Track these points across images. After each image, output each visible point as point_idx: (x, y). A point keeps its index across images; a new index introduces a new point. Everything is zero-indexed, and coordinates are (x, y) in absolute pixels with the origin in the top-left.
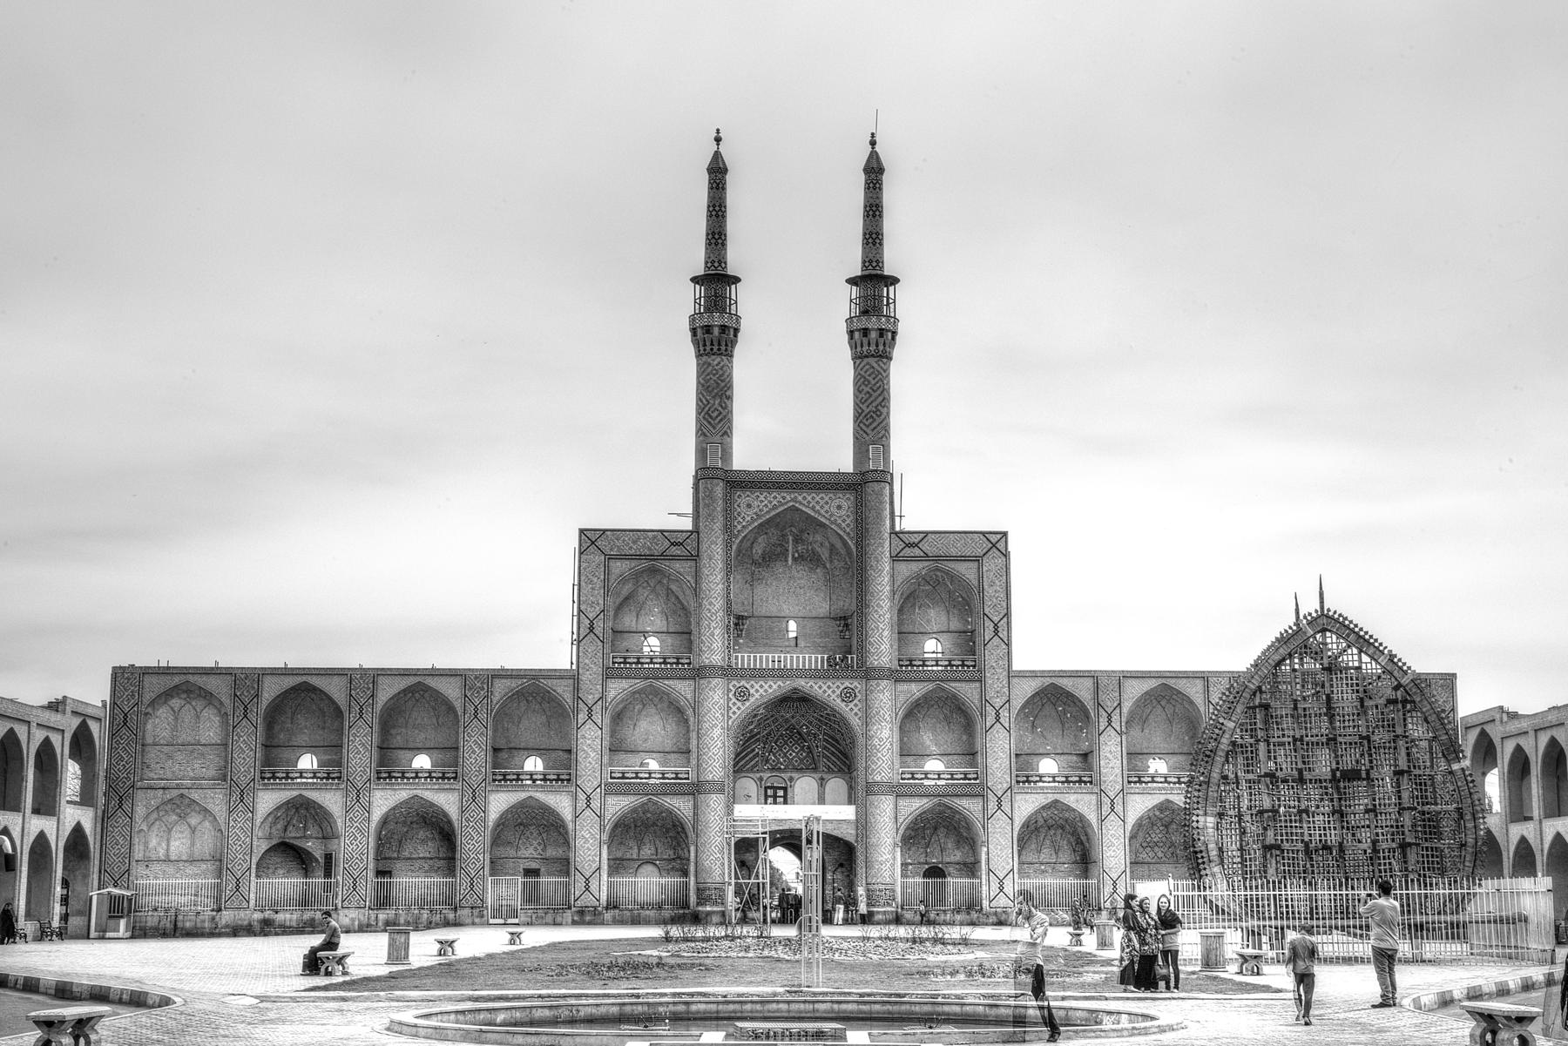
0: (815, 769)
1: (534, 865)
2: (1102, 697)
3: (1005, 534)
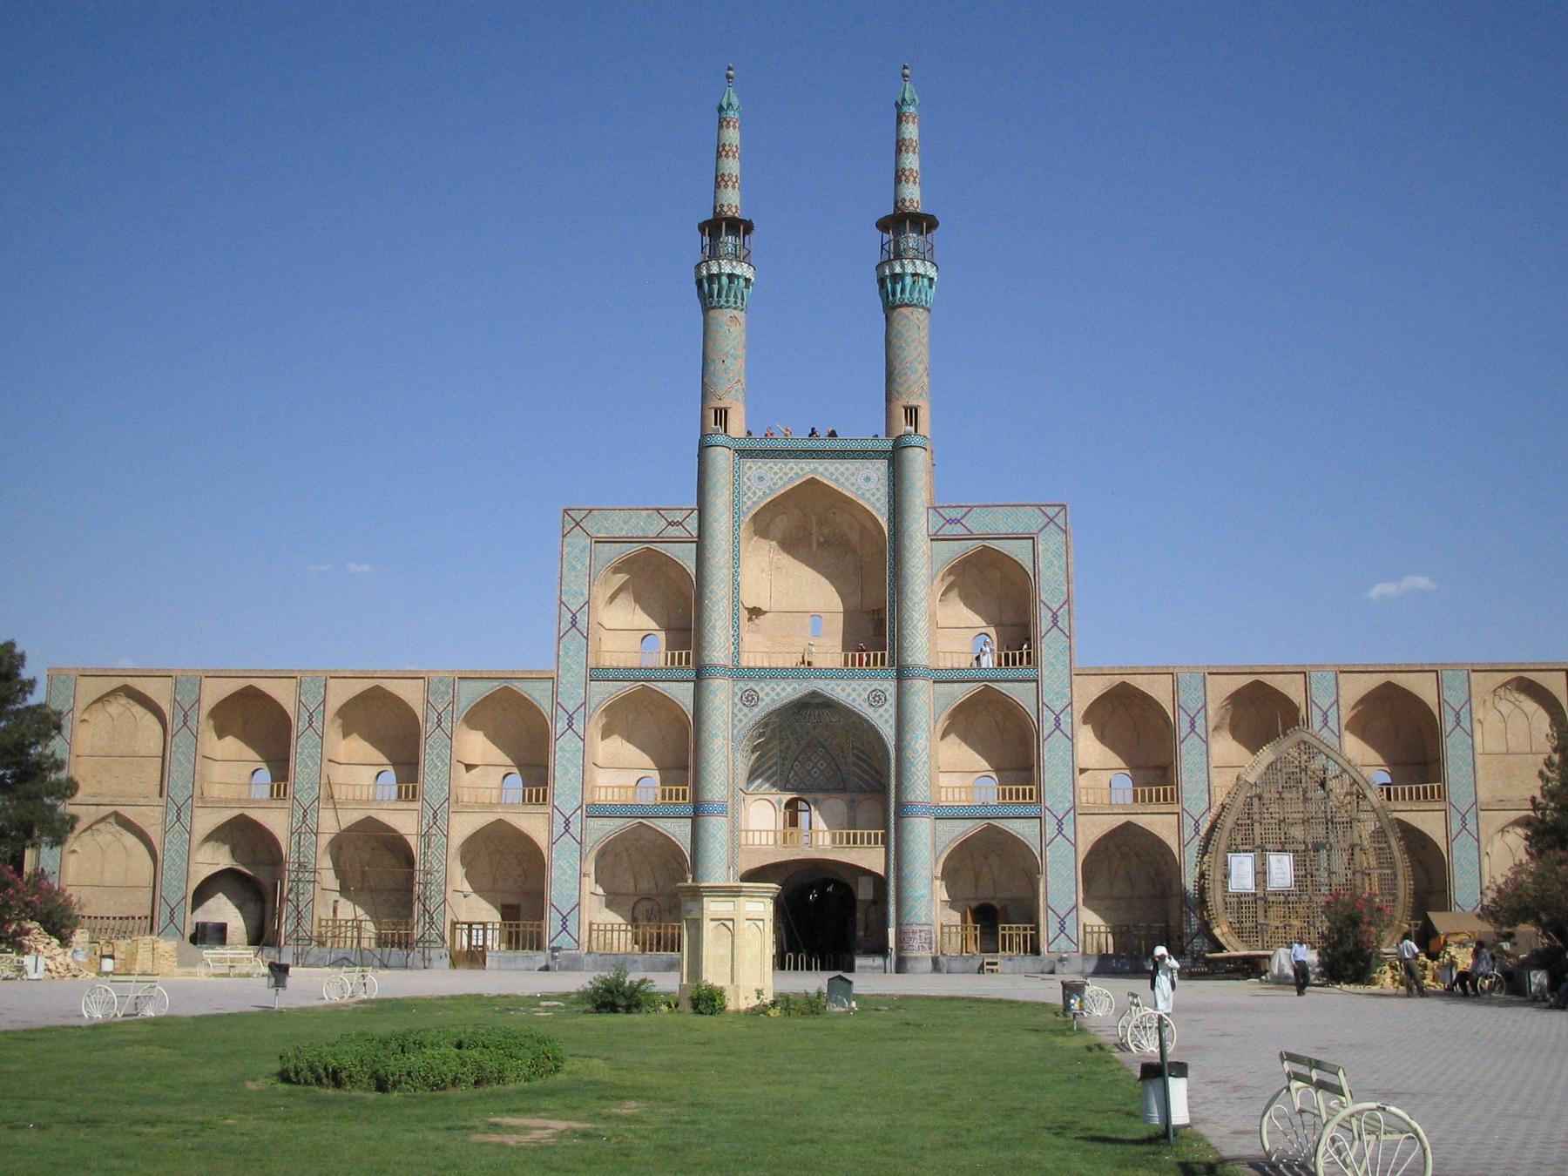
2: (1183, 698)
3: (1064, 506)
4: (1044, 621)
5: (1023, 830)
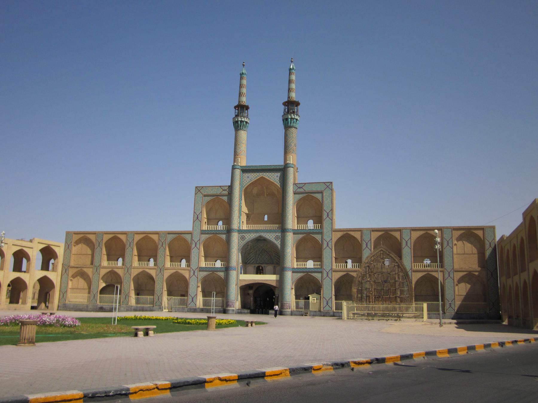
0: (273, 263)
1: (183, 293)
2: (364, 237)
4: (325, 216)
5: (318, 276)
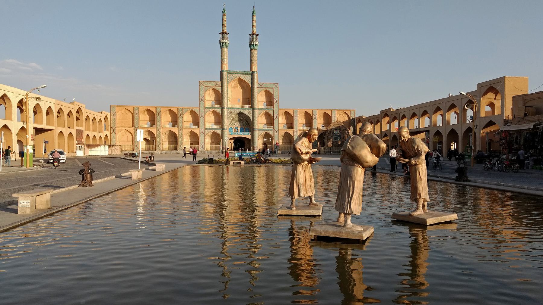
4: (275, 102)
5: (271, 132)
